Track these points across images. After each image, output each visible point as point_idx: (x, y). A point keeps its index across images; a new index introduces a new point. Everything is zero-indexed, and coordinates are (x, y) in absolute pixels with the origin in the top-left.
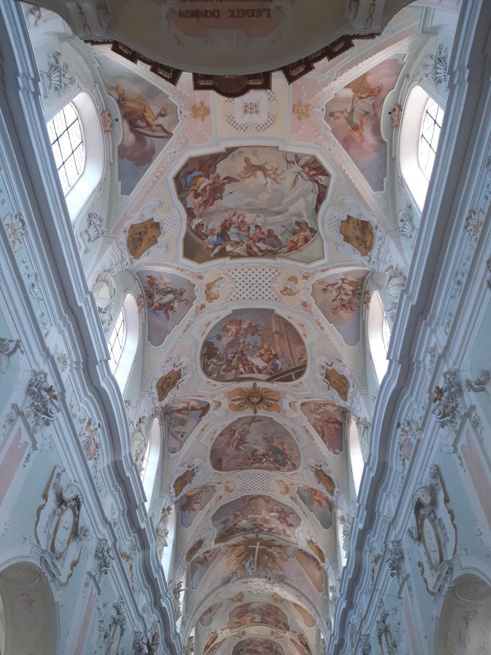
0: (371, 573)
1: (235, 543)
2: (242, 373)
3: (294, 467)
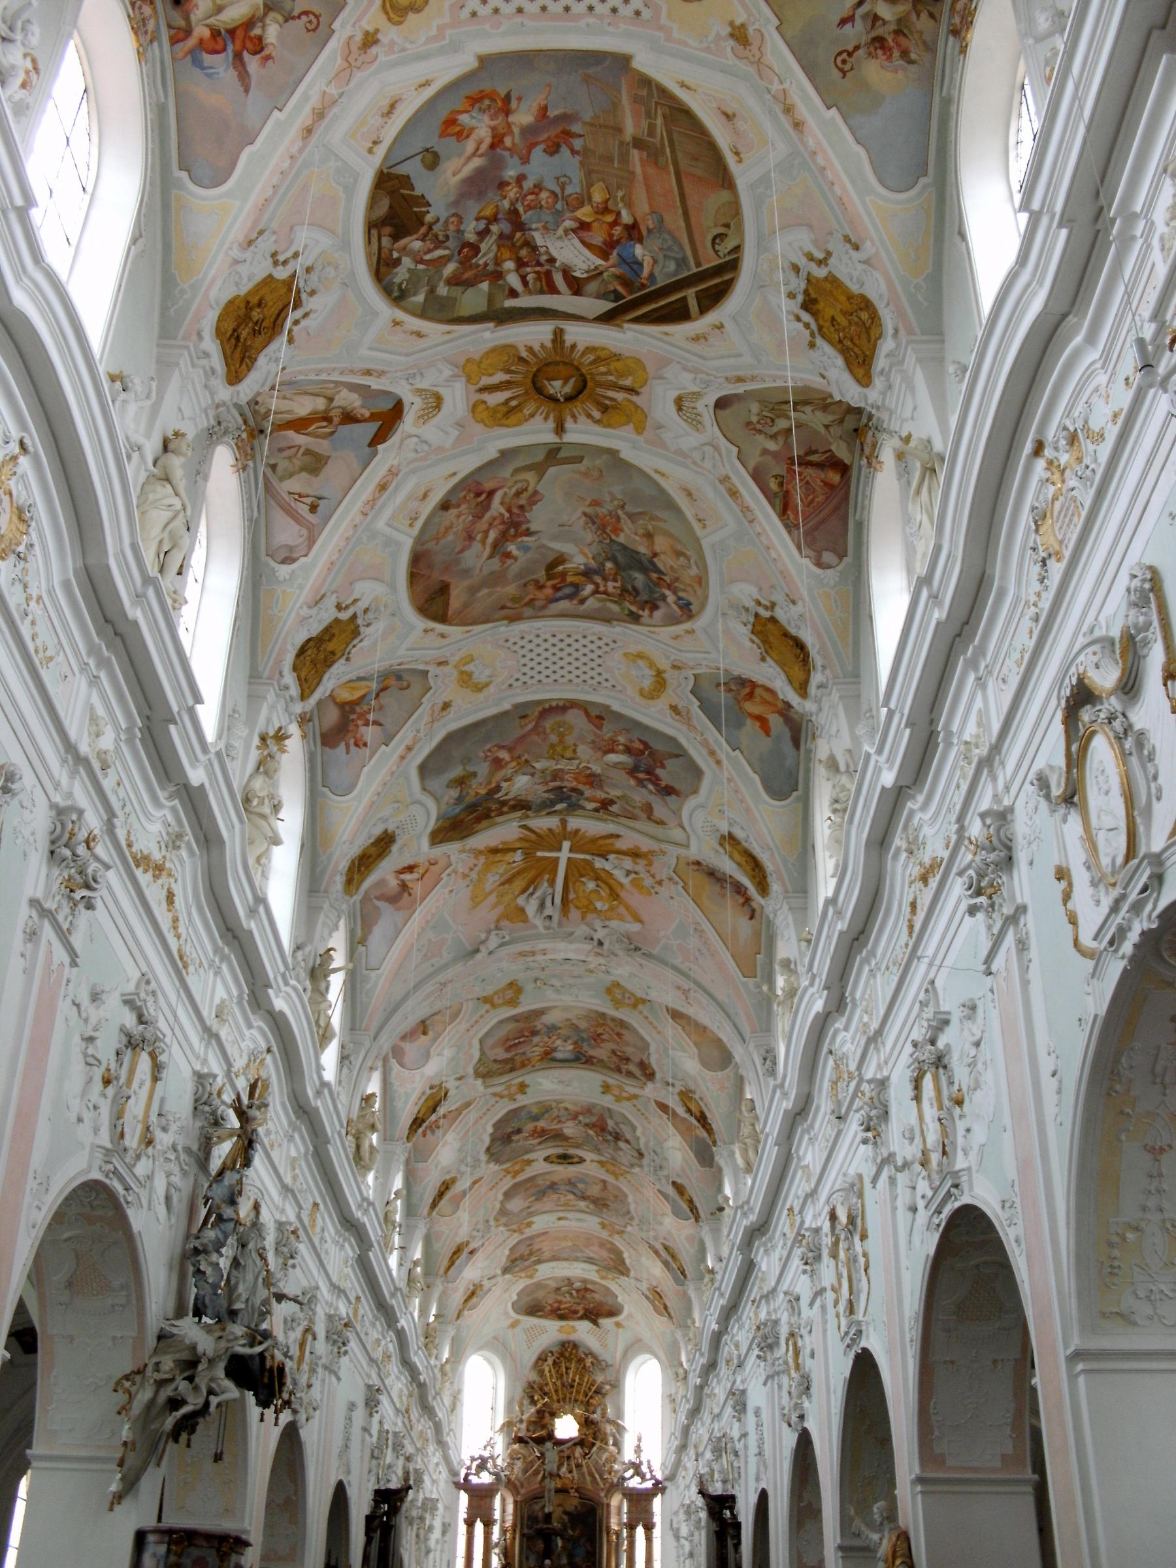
0: (906, 909)
1: (493, 843)
2: (513, 294)
3: (687, 611)
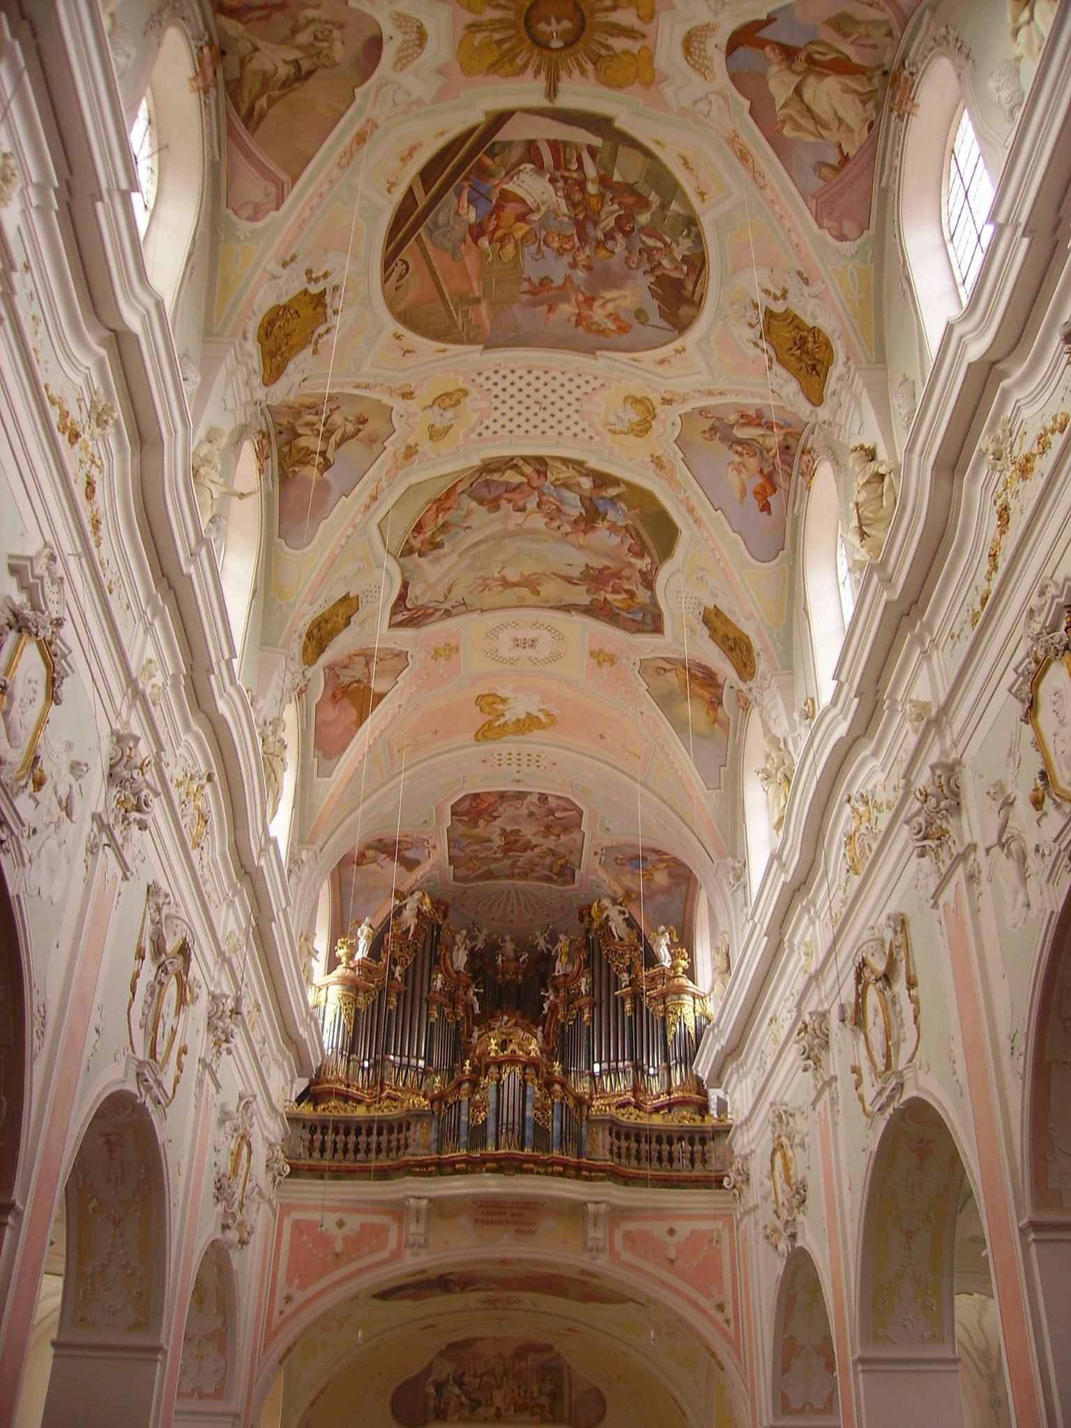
2: (593, 152)
